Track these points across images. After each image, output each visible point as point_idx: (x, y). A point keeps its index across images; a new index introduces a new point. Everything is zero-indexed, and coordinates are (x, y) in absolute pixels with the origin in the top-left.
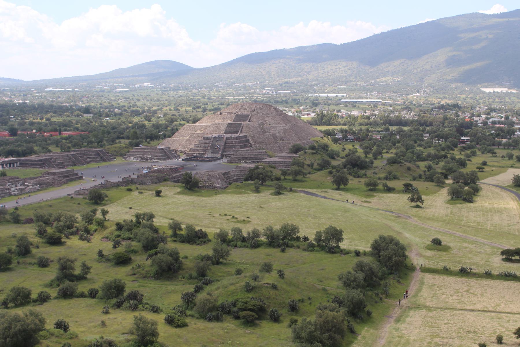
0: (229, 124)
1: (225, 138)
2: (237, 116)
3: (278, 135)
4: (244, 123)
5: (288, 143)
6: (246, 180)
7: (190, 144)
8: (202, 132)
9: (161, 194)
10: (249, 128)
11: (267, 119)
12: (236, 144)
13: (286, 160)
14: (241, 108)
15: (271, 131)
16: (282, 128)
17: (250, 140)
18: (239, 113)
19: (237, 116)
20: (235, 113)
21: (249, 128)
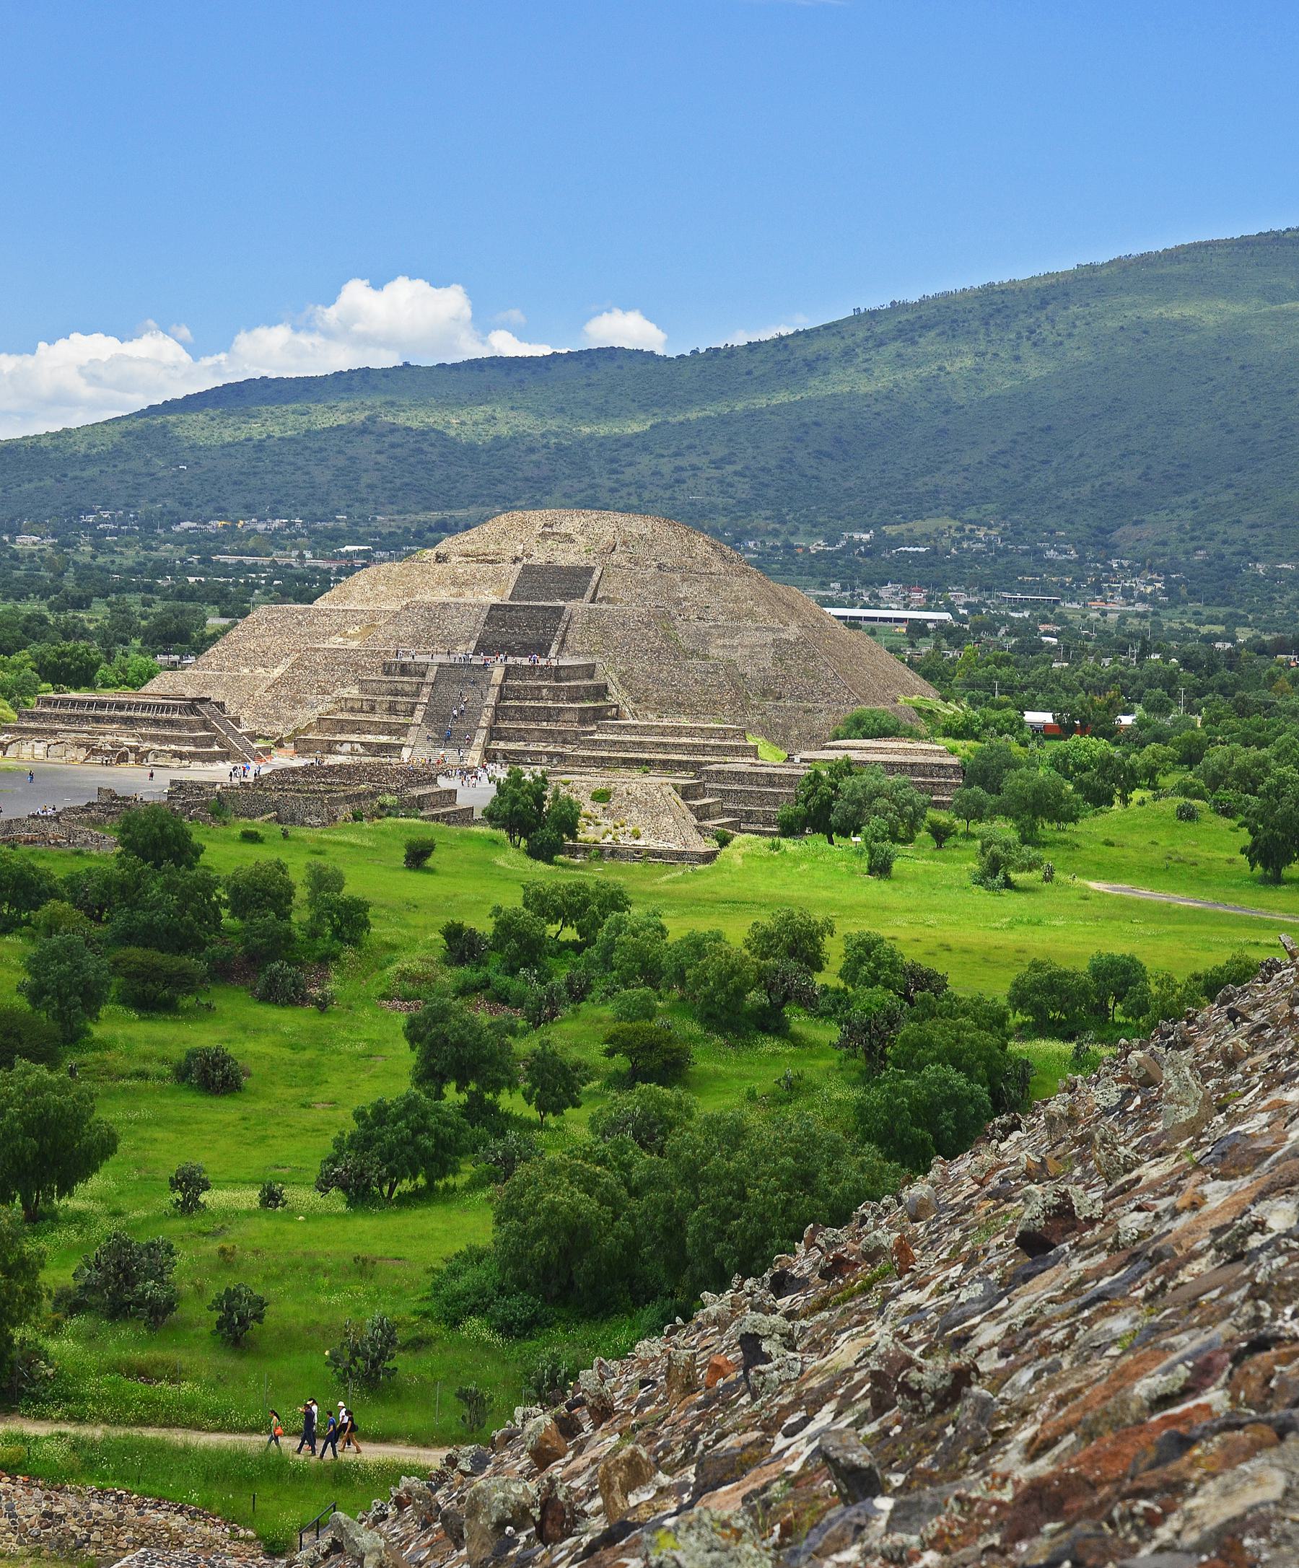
0: (494, 607)
1: (498, 674)
2: (527, 570)
3: (749, 670)
4: (575, 606)
5: (807, 711)
6: (790, 829)
7: (296, 702)
8: (354, 644)
9: (430, 862)
10: (605, 633)
11: (684, 590)
12: (556, 698)
13: (920, 759)
14: (542, 535)
15: (713, 651)
16: (770, 637)
17: (612, 689)
18: (539, 558)
19: (527, 570)
20: (516, 560)
21: (605, 633)
